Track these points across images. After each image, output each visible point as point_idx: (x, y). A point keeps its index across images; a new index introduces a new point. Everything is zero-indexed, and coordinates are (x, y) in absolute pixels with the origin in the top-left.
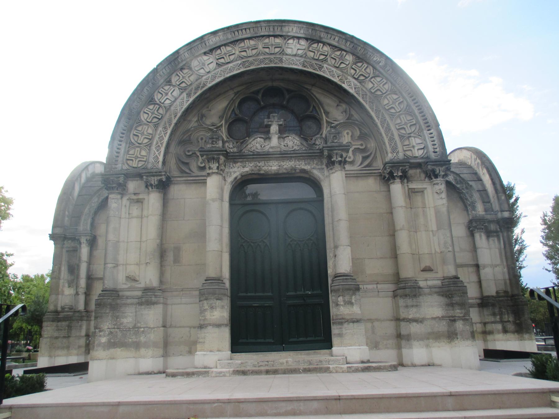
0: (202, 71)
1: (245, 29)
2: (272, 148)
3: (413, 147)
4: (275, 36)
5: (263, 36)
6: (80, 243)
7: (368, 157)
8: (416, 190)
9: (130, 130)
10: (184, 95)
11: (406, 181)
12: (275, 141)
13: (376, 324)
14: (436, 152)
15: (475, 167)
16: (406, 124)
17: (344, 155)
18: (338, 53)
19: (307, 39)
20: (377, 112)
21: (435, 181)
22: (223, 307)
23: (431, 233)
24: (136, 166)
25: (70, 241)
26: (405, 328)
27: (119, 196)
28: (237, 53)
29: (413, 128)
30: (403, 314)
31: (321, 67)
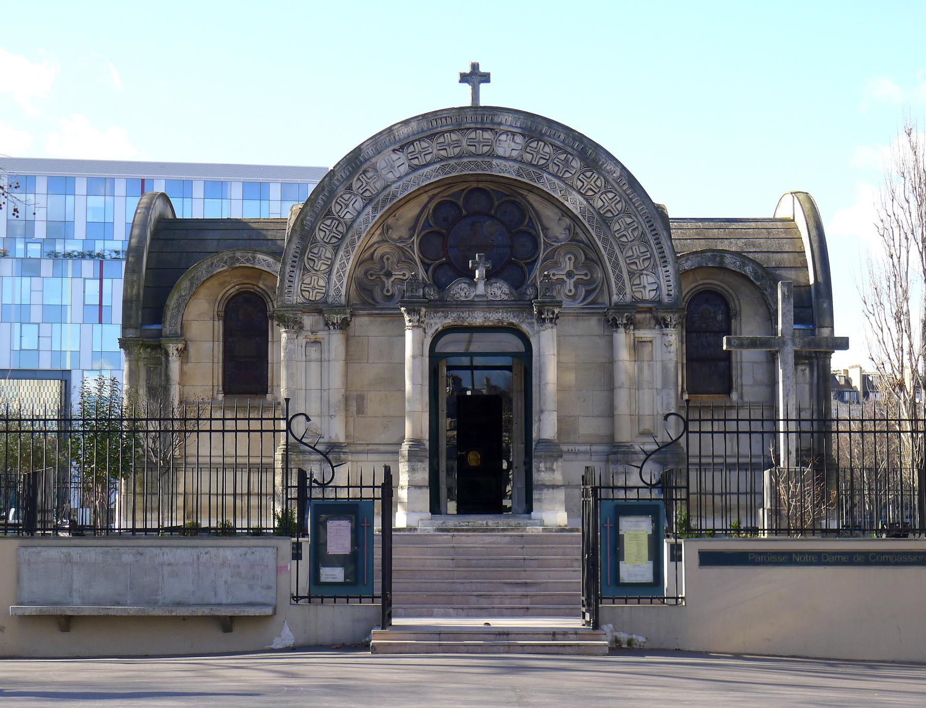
0: (390, 176)
5: (469, 129)
6: (167, 354)
7: (594, 290)
9: (303, 253)
10: (369, 209)
11: (632, 327)
12: (481, 289)
16: (638, 257)
17: (556, 311)
18: (563, 157)
19: (524, 136)
20: (605, 241)
22: (424, 469)
25: (149, 350)
28: (435, 151)
29: (647, 263)
31: (540, 177)
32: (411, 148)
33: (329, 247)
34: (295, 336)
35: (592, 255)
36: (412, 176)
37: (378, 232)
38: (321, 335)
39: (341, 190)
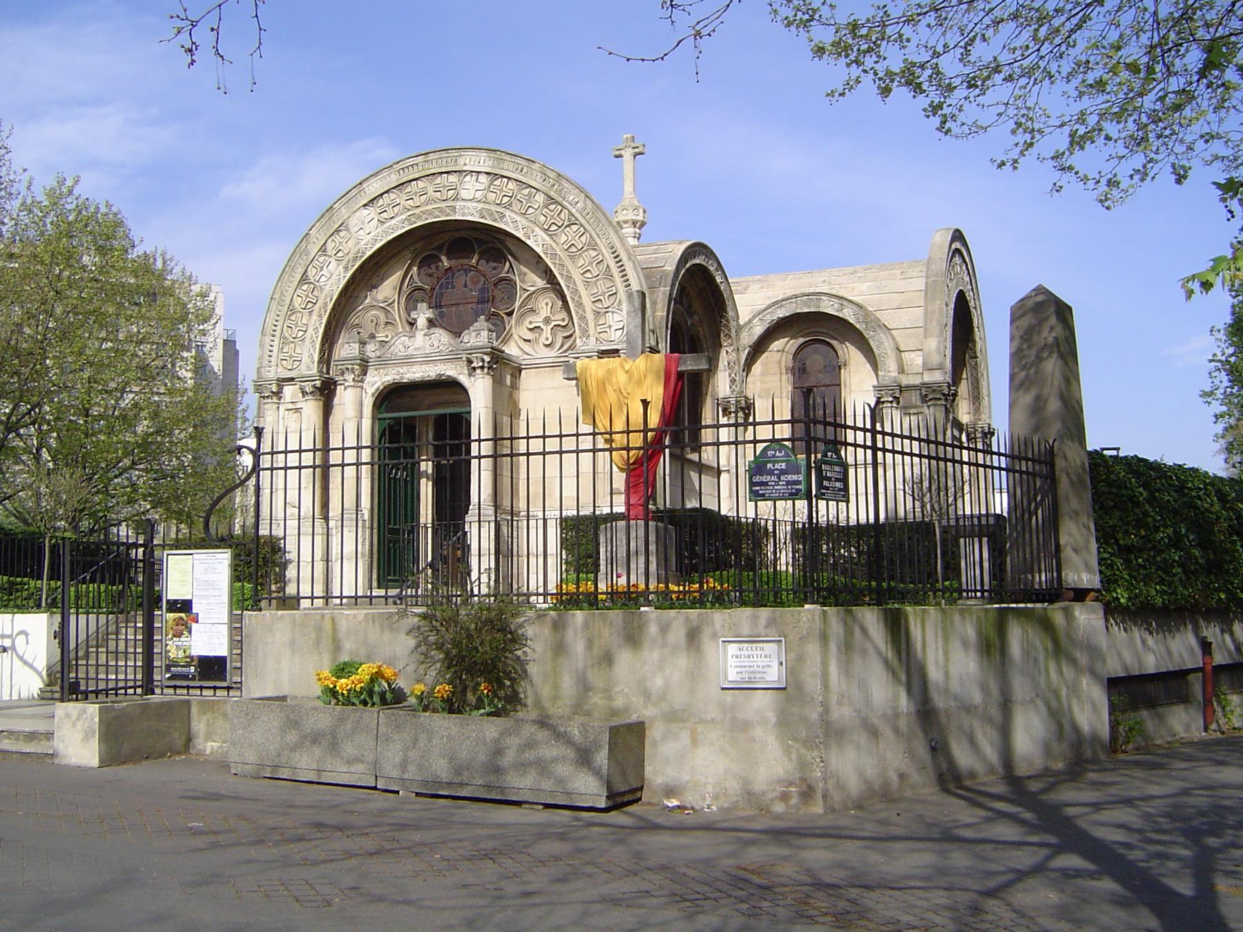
18: (526, 191)
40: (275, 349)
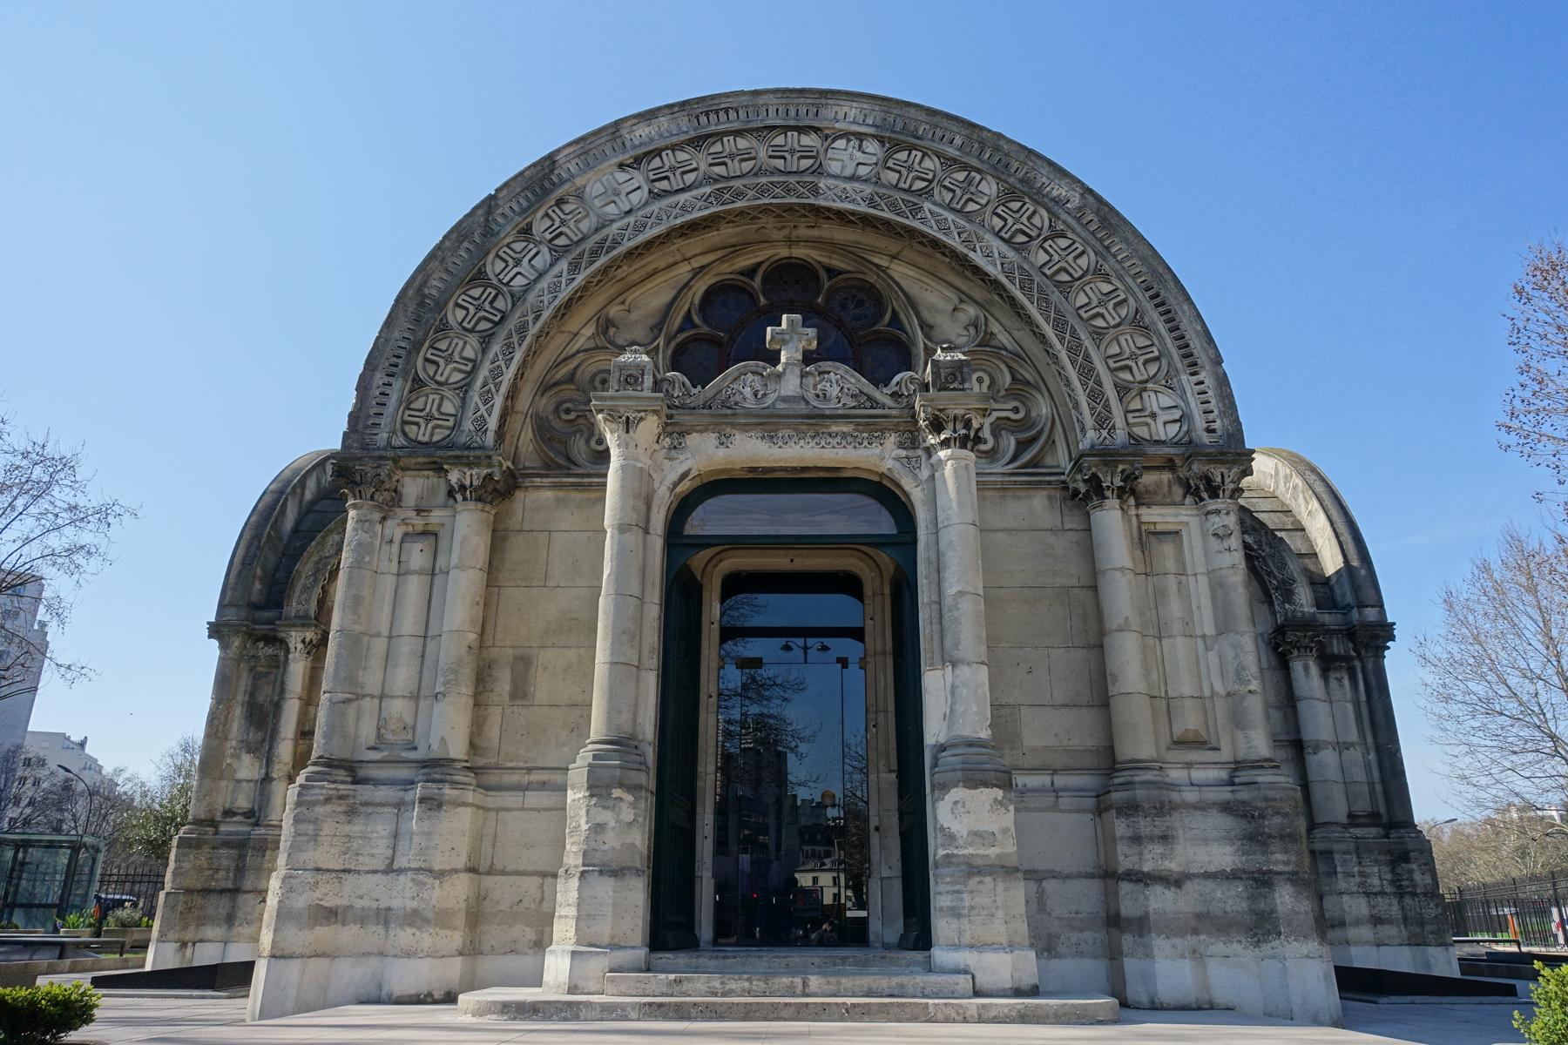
0: (611, 209)
1: (726, 110)
2: (786, 399)
3: (1153, 415)
4: (801, 130)
5: (772, 128)
6: (288, 651)
7: (1034, 440)
8: (1159, 528)
9: (417, 346)
10: (563, 265)
11: (1132, 501)
13: (1050, 886)
14: (1214, 431)
15: (1287, 498)
18: (961, 176)
19: (881, 141)
20: (1060, 325)
21: (1212, 505)
23: (1200, 642)
24: (426, 439)
26: (1130, 901)
27: (377, 516)
28: (703, 167)
29: (1152, 369)
30: (1126, 859)
31: (916, 210)
32: (656, 162)
33: (473, 340)
34: (377, 516)
35: (1029, 375)
36: (655, 207)
37: (589, 331)
38: (437, 516)
39: (507, 232)
40: (393, 401)
